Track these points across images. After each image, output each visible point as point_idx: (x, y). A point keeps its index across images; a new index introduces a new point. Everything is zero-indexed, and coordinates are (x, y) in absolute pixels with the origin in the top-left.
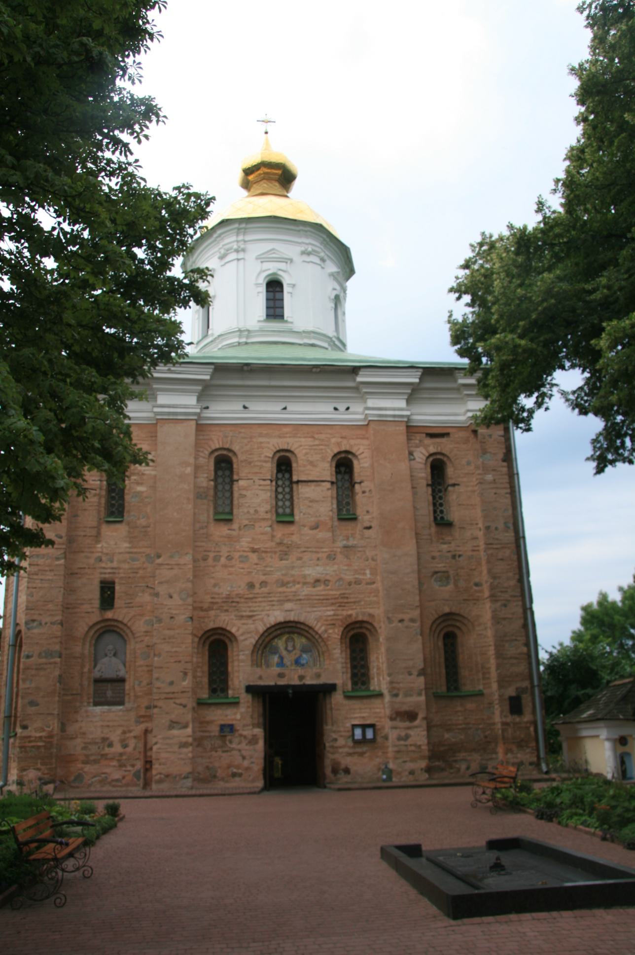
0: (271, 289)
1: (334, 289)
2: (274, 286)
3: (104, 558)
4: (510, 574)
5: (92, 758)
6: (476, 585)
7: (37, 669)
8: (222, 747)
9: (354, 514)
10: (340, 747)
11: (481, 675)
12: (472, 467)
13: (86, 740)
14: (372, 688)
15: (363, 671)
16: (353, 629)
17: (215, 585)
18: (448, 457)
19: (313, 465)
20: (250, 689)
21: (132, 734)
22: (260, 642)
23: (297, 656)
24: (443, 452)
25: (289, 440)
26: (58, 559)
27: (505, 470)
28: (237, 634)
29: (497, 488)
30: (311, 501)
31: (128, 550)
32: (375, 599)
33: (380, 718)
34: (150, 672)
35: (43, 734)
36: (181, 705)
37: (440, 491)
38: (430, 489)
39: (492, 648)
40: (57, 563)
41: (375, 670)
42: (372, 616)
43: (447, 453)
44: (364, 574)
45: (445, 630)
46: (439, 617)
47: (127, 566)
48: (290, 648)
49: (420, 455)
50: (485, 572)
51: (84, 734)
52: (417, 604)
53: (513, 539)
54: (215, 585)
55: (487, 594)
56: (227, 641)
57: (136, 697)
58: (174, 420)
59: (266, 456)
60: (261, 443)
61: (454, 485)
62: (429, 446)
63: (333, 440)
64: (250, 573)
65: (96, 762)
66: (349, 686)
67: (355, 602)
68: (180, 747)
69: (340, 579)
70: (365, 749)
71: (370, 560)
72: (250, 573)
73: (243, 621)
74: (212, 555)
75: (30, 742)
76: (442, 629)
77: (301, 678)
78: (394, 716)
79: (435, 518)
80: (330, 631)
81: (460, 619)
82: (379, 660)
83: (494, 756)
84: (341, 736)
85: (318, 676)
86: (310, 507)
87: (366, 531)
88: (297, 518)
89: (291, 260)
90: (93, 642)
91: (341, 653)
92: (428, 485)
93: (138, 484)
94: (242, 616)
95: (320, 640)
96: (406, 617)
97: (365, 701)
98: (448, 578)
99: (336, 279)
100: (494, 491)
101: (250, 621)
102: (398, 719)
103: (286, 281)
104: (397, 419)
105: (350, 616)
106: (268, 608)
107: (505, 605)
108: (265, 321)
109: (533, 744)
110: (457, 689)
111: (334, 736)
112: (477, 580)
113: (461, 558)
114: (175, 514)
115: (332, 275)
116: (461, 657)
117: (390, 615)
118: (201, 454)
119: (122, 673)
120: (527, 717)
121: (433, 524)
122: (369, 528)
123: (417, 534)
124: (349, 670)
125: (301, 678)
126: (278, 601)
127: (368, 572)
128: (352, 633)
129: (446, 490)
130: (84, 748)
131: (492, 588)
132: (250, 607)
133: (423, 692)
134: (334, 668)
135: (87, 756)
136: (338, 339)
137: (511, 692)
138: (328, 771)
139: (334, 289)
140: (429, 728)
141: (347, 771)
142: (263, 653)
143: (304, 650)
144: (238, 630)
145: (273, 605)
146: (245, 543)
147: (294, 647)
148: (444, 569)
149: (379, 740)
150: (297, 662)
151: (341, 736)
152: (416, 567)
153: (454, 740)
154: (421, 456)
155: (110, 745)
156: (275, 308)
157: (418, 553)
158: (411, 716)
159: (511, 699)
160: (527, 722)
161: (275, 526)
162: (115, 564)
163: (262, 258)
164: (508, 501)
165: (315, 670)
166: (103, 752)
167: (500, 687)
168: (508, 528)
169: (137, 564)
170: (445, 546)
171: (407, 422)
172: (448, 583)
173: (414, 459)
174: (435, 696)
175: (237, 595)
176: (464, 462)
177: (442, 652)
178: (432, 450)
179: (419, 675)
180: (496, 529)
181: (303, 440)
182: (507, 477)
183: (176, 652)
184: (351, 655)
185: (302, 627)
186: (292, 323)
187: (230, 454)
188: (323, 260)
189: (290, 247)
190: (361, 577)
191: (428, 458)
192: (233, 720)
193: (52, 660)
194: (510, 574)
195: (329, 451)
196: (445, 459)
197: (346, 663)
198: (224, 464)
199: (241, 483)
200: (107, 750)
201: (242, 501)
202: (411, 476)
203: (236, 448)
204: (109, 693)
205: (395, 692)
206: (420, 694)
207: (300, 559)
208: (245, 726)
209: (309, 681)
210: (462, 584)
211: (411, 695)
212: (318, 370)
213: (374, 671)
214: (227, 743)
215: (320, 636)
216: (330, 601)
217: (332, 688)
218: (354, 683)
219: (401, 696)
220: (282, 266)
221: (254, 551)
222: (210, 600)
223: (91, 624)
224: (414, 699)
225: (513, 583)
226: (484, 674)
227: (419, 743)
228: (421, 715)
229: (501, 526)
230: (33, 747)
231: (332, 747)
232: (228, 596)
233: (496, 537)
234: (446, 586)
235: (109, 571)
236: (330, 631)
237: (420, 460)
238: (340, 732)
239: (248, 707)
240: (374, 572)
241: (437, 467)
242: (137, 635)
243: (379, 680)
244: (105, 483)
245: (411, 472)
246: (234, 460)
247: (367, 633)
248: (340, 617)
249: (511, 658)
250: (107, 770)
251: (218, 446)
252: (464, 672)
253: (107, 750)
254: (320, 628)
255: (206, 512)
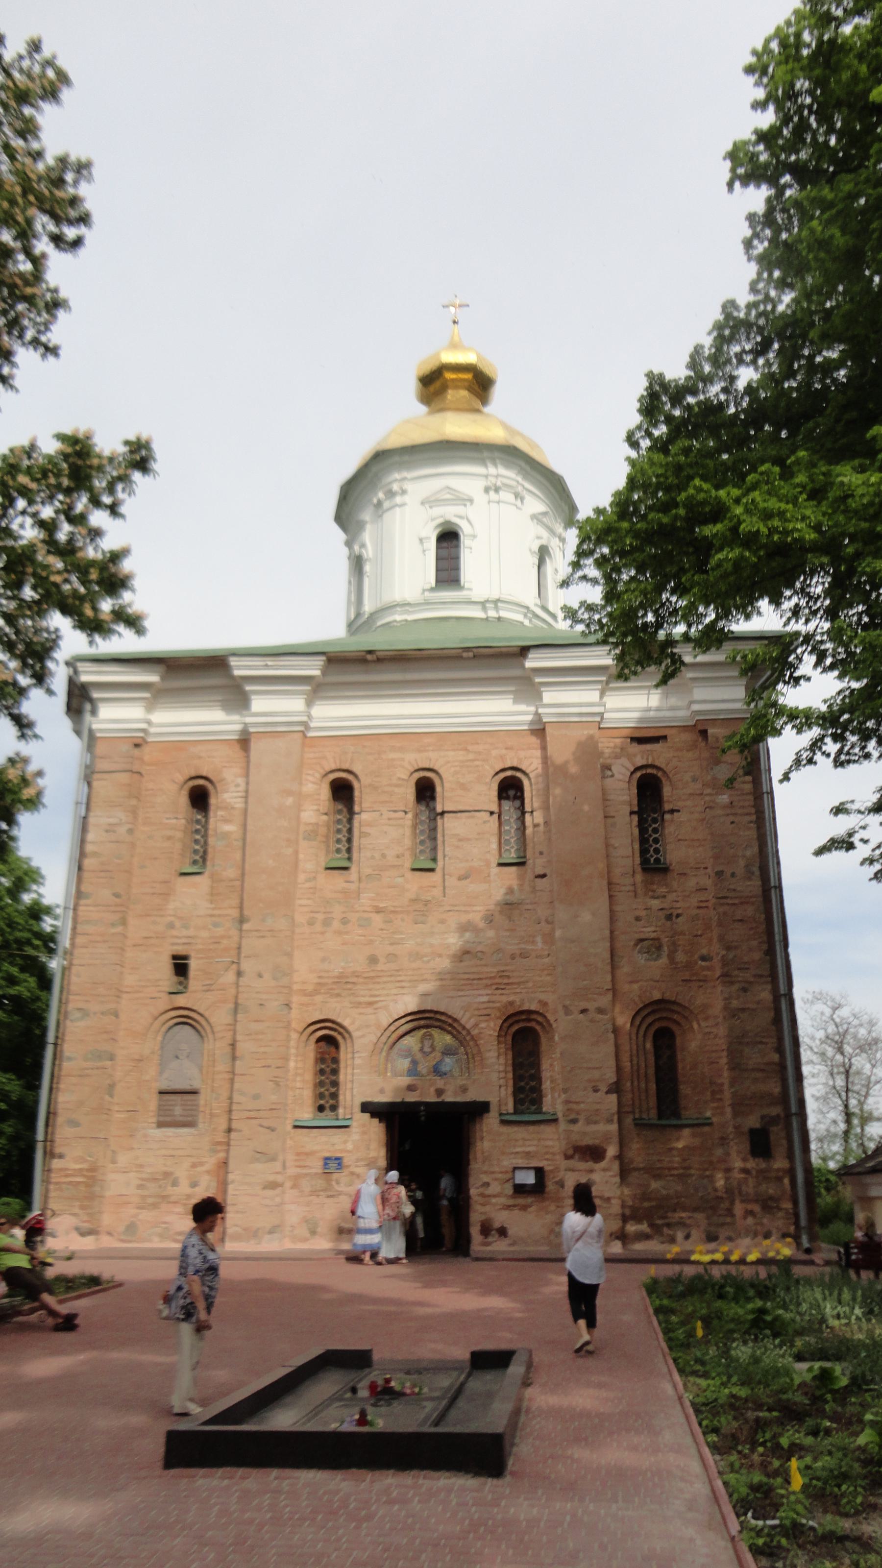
0: (445, 544)
1: (538, 538)
2: (449, 537)
3: (178, 924)
4: (754, 943)
5: (150, 1200)
6: (703, 958)
7: (80, 1076)
8: (325, 1190)
9: (525, 857)
10: (495, 1196)
11: (708, 1096)
12: (699, 785)
13: (144, 1176)
14: (544, 1109)
15: (533, 1084)
16: (517, 1022)
17: (324, 960)
18: (664, 772)
19: (469, 791)
20: (366, 1107)
21: (204, 1168)
22: (384, 1039)
23: (438, 1059)
24: (657, 763)
25: (431, 755)
26: (113, 925)
27: (748, 787)
28: (351, 1028)
29: (736, 814)
30: (460, 840)
31: (210, 912)
32: (548, 978)
33: (554, 1154)
34: (232, 1081)
35: (84, 1166)
36: (268, 1128)
37: (655, 821)
38: (635, 818)
39: (725, 1054)
40: (113, 930)
41: (548, 1083)
42: (544, 1004)
43: (663, 766)
44: (533, 942)
45: (657, 1026)
46: (646, 1006)
47: (204, 934)
48: (427, 1049)
49: (622, 770)
50: (715, 940)
51: (141, 1166)
52: (610, 987)
53: (758, 891)
54: (324, 960)
55: (718, 973)
56: (339, 1038)
57: (212, 1115)
58: (273, 734)
59: (399, 779)
60: (393, 760)
61: (672, 811)
62: (635, 755)
63: (494, 753)
64: (371, 942)
65: (155, 1206)
66: (510, 1107)
67: (519, 983)
68: (264, 1188)
69: (499, 950)
70: (530, 1200)
71: (543, 924)
72: (371, 942)
73: (362, 1010)
74: (320, 917)
75: (67, 1176)
76: (650, 1025)
77: (440, 1092)
78: (571, 1152)
79: (645, 862)
80: (483, 1025)
81: (675, 1008)
82: (551, 1068)
83: (728, 1220)
84: (496, 1179)
85: (464, 1089)
86: (458, 847)
87: (539, 880)
88: (440, 863)
89: (471, 501)
90: (160, 1038)
91: (498, 1057)
92: (632, 813)
93: (226, 821)
94: (360, 1003)
95: (468, 1038)
96: (591, 1006)
97: (531, 1128)
98: (659, 948)
99: (540, 522)
100: (732, 818)
101: (370, 1010)
102: (577, 1156)
103: (465, 529)
104: (584, 719)
105: (511, 1003)
106: (394, 991)
107: (745, 990)
108: (432, 590)
109: (788, 1205)
110: (677, 1114)
111: (485, 1178)
112: (704, 951)
113: (680, 919)
114: (271, 862)
115: (534, 517)
116: (680, 1066)
117: (567, 1003)
118: (310, 778)
119: (196, 1084)
120: (780, 1163)
121: (639, 869)
122: (543, 876)
123: (610, 883)
124: (511, 1083)
125: (440, 1092)
126: (410, 981)
127: (539, 939)
128: (516, 1027)
129: (663, 819)
130: (140, 1187)
131: (725, 962)
132: (370, 990)
133: (616, 1117)
134: (489, 1080)
135: (143, 1197)
136: (545, 609)
137: (753, 1121)
138: (475, 1231)
139: (538, 538)
140: (624, 1173)
141: (502, 1232)
142: (388, 1054)
143: (448, 1052)
144: (353, 1023)
145: (403, 987)
146: (366, 900)
147: (433, 1048)
148: (653, 935)
149: (550, 1186)
150: (436, 1070)
151: (496, 1179)
152: (607, 932)
153: (664, 1192)
154: (623, 770)
155: (175, 1183)
156: (448, 572)
157: (612, 911)
158: (594, 1153)
159: (753, 1132)
160: (778, 1170)
161: (410, 875)
162: (191, 932)
163: (428, 502)
164: (753, 833)
165: (460, 1082)
166: (164, 1193)
167: (736, 1114)
168: (753, 873)
169: (220, 931)
170: (655, 903)
171: (599, 723)
172: (659, 957)
173: (612, 776)
174: (636, 1125)
175: (354, 972)
176: (687, 777)
177: (652, 1059)
178: (640, 761)
179: (607, 1093)
180: (733, 875)
181: (451, 753)
182: (751, 798)
183: (265, 1053)
184: (514, 1059)
185: (443, 1018)
186: (470, 589)
187: (350, 777)
188: (517, 495)
189: (467, 479)
190: (530, 947)
191: (632, 773)
192: (341, 1151)
193: (100, 1064)
194: (754, 943)
195: (487, 767)
196: (660, 774)
197: (506, 1072)
198: (342, 791)
199: (364, 816)
200: (170, 1190)
201: (363, 841)
202: (605, 800)
203: (356, 769)
204: (178, 1110)
205: (573, 1116)
206: (610, 1121)
207: (442, 922)
208: (358, 1160)
209: (449, 1098)
210: (680, 957)
211: (596, 1123)
212: (471, 654)
213: (546, 1085)
214: (334, 1183)
215: (469, 1033)
216: (484, 981)
217: (481, 1108)
218: (516, 1103)
219: (580, 1123)
220: (460, 510)
221: (378, 911)
222: (317, 980)
223: (156, 1013)
224: (602, 1127)
225: (757, 956)
226: (713, 1093)
227: (607, 1195)
228: (612, 1151)
229: (740, 870)
230: (70, 1183)
231: (482, 1195)
232: (341, 976)
233: (732, 887)
234: (656, 960)
235: (184, 940)
236: (483, 1025)
237: (621, 777)
238: (493, 1173)
239: (364, 1133)
240: (549, 938)
241: (649, 788)
242: (216, 1029)
243: (552, 1098)
244: (183, 821)
245: (603, 794)
246: (356, 785)
247: (538, 1028)
248: (498, 1005)
249: (753, 1070)
250: (168, 1219)
251: (333, 767)
252: (685, 1089)
253: (170, 1190)
254: (467, 1020)
255: (311, 858)
